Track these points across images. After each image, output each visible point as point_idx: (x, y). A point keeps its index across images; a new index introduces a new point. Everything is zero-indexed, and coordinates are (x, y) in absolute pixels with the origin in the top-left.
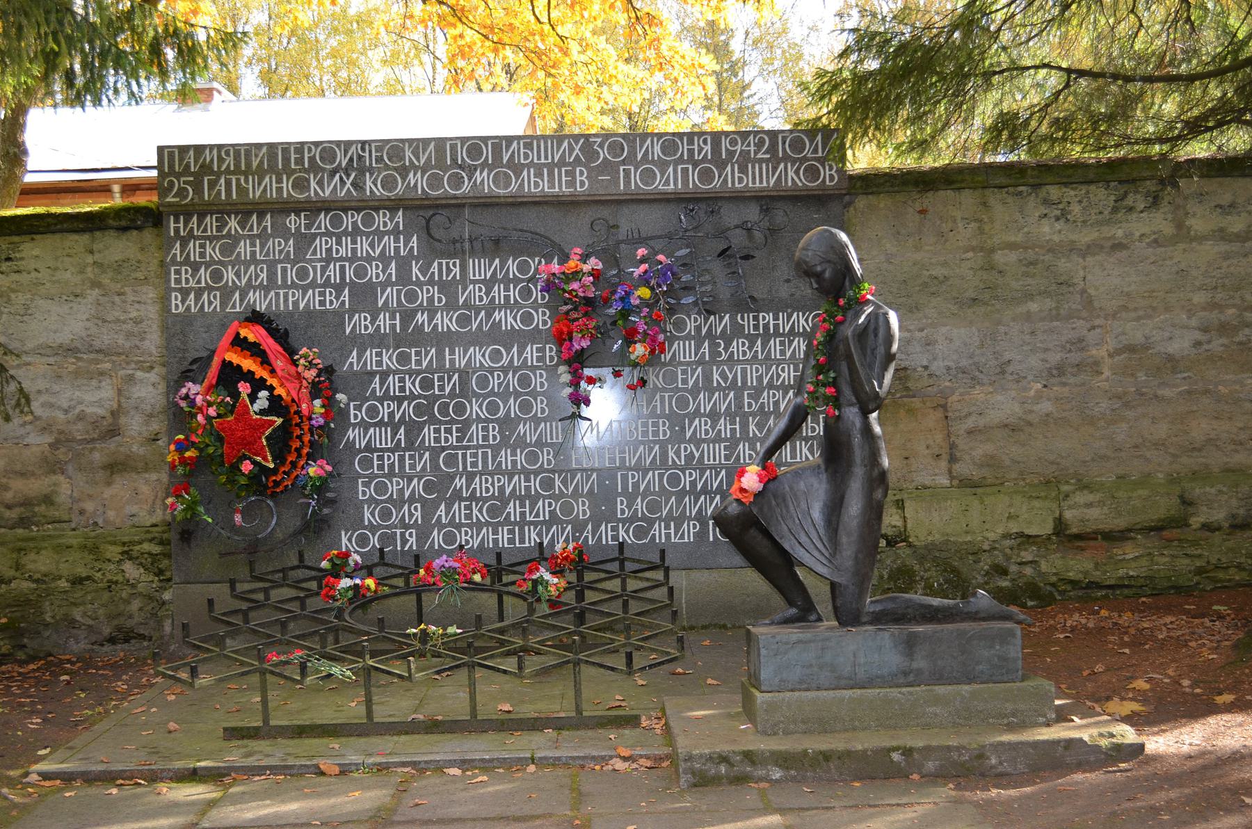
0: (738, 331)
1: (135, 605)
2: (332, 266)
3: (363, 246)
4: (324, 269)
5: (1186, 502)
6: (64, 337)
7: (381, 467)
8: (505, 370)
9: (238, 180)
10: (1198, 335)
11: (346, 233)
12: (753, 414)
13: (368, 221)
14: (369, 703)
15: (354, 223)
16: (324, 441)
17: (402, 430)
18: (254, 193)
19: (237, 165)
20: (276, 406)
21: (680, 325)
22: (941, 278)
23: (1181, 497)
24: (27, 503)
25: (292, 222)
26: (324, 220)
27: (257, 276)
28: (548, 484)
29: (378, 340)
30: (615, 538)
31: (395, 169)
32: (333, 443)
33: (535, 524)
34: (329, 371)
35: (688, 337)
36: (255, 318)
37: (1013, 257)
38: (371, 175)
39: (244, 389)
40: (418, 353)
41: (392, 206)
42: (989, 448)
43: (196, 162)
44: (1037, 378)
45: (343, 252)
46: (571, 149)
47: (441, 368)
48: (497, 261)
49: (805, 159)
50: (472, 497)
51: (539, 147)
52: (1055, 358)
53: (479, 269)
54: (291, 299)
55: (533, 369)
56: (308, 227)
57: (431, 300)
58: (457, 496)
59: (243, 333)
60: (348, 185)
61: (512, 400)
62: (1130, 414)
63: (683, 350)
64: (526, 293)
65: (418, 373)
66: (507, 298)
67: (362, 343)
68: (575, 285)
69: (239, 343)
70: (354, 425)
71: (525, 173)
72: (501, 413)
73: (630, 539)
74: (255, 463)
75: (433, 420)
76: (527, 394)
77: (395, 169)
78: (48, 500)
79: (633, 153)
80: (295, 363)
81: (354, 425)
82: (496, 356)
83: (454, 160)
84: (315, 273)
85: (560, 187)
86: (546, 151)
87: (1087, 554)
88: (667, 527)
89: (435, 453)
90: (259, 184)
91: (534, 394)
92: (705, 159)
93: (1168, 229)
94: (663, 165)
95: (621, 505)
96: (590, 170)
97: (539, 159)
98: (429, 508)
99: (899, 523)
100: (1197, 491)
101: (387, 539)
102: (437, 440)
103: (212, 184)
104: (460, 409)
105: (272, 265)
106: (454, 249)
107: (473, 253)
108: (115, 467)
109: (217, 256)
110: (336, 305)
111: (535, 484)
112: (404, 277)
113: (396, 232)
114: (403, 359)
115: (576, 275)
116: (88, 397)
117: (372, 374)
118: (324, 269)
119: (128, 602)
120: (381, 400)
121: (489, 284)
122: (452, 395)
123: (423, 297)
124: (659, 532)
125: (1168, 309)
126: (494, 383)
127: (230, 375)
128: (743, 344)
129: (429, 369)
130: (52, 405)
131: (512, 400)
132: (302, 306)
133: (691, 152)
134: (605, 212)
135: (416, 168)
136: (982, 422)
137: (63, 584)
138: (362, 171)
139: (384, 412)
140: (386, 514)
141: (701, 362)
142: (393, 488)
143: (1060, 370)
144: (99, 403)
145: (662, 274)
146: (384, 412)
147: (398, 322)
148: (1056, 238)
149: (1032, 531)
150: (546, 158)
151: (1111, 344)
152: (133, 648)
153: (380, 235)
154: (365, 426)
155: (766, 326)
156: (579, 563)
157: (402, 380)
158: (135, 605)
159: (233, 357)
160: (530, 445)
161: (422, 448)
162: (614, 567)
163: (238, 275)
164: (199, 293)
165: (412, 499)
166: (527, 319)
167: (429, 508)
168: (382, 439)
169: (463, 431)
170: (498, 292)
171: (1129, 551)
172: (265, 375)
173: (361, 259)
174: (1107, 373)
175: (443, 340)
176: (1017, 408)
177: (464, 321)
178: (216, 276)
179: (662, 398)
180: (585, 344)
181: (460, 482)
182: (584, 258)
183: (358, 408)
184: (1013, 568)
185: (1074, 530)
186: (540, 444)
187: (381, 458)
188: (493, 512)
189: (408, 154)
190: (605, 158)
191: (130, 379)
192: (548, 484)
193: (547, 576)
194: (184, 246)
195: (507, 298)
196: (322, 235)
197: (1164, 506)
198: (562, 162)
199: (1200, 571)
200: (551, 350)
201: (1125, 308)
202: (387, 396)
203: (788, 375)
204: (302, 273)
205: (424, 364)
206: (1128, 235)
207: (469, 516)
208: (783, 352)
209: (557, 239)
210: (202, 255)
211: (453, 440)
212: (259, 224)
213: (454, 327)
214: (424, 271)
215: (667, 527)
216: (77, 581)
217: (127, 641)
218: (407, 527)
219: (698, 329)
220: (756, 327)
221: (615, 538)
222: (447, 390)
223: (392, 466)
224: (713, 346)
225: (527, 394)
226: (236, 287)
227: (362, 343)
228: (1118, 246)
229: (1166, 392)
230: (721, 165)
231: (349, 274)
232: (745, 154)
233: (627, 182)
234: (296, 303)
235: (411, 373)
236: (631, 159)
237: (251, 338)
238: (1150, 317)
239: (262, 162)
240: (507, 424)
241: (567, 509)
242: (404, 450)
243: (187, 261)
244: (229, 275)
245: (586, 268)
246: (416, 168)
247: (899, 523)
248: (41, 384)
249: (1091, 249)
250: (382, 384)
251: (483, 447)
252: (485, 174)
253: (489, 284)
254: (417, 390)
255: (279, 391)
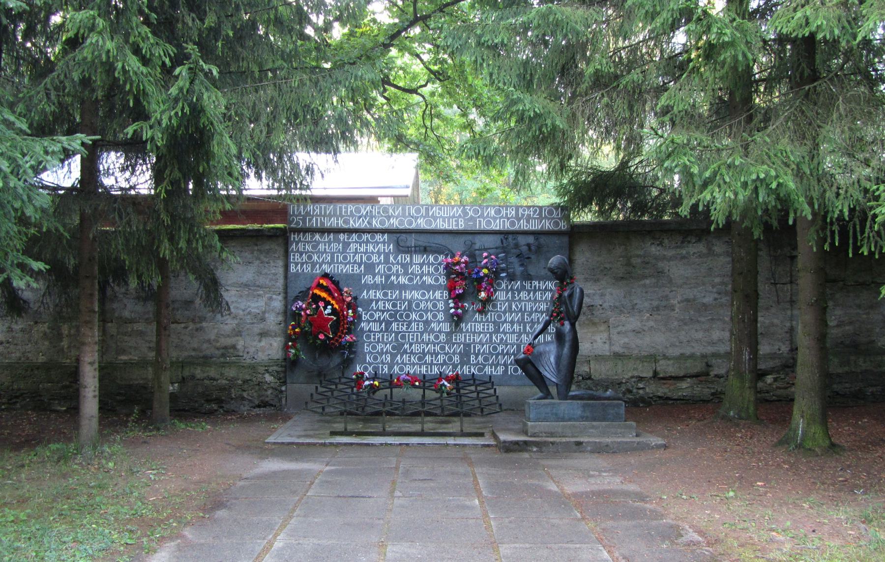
0: (523, 288)
1: (269, 392)
3: (370, 248)
4: (354, 257)
5: (708, 366)
6: (244, 280)
7: (374, 339)
8: (427, 301)
10: (716, 296)
11: (363, 242)
12: (529, 323)
13: (373, 238)
14: (424, 396)
16: (352, 327)
18: (327, 224)
19: (321, 212)
20: (334, 312)
21: (499, 285)
23: (707, 363)
24: (225, 348)
25: (342, 237)
26: (355, 236)
28: (443, 348)
29: (375, 286)
30: (470, 372)
32: (355, 329)
33: (437, 365)
34: (355, 298)
35: (503, 290)
36: (326, 276)
37: (639, 260)
39: (321, 304)
41: (383, 232)
42: (626, 340)
44: (648, 311)
47: (400, 299)
49: (553, 218)
50: (412, 353)
52: (655, 303)
53: (418, 259)
55: (438, 300)
56: (348, 239)
57: (397, 271)
58: (405, 352)
59: (321, 281)
62: (686, 328)
63: (500, 296)
64: (437, 270)
65: (391, 300)
67: (369, 287)
68: (457, 267)
69: (320, 286)
72: (425, 318)
73: (476, 372)
74: (325, 335)
75: (396, 320)
78: (234, 347)
79: (483, 214)
80: (342, 295)
82: (423, 295)
83: (409, 214)
84: (350, 257)
85: (452, 226)
87: (666, 386)
89: (397, 333)
91: (438, 311)
92: (512, 217)
93: (705, 251)
94: (495, 219)
95: (473, 358)
96: (465, 220)
98: (393, 356)
99: (588, 370)
100: (714, 361)
101: (376, 369)
102: (398, 328)
103: (310, 220)
104: (408, 316)
105: (333, 254)
106: (408, 250)
107: (415, 252)
108: (263, 334)
109: (310, 249)
111: (437, 348)
112: (387, 261)
113: (384, 242)
114: (385, 294)
115: (458, 263)
116: (253, 305)
117: (372, 301)
118: (354, 257)
119: (266, 390)
121: (422, 265)
122: (405, 310)
123: (394, 269)
124: (488, 370)
125: (704, 284)
126: (422, 306)
127: (316, 299)
129: (396, 299)
130: (237, 308)
133: (507, 214)
134: (470, 237)
136: (624, 329)
137: (240, 382)
138: (372, 217)
139: (376, 316)
140: (375, 358)
141: (507, 300)
142: (379, 348)
143: (658, 308)
144: (257, 308)
145: (492, 264)
146: (376, 316)
148: (658, 253)
149: (644, 375)
151: (679, 298)
152: (272, 408)
153: (378, 243)
154: (369, 322)
155: (535, 287)
156: (455, 379)
157: (384, 303)
158: (269, 392)
159: (317, 291)
161: (392, 332)
162: (471, 382)
163: (318, 257)
164: (302, 264)
165: (387, 352)
166: (437, 280)
167: (393, 356)
168: (375, 327)
169: (409, 325)
170: (425, 269)
171: (684, 385)
172: (330, 299)
174: (677, 310)
175: (402, 287)
176: (639, 324)
177: (411, 280)
178: (310, 258)
180: (461, 291)
181: (406, 346)
182: (461, 256)
183: (366, 314)
184: (635, 391)
185: (661, 376)
186: (440, 332)
187: (374, 335)
188: (420, 359)
189: (391, 211)
191: (270, 299)
192: (443, 348)
193: (446, 383)
194: (297, 245)
197: (698, 367)
198: (454, 216)
199: (713, 394)
200: (446, 294)
201: (685, 283)
202: (378, 310)
203: (543, 307)
204: (345, 258)
206: (688, 253)
207: (410, 360)
209: (450, 247)
210: (304, 249)
211: (404, 329)
213: (407, 282)
214: (395, 258)
216: (245, 381)
217: (265, 407)
218: (384, 364)
219: (507, 286)
221: (470, 372)
223: (379, 338)
224: (513, 294)
226: (317, 262)
227: (369, 287)
228: (683, 257)
229: (703, 319)
230: (519, 220)
231: (364, 259)
232: (529, 215)
233: (480, 225)
234: (342, 270)
235: (388, 300)
236: (482, 216)
237: (325, 284)
238: (695, 287)
240: (427, 323)
241: (450, 359)
243: (298, 251)
244: (315, 257)
245: (463, 260)
247: (588, 370)
248: (234, 299)
249: (670, 259)
253: (422, 265)
255: (336, 306)
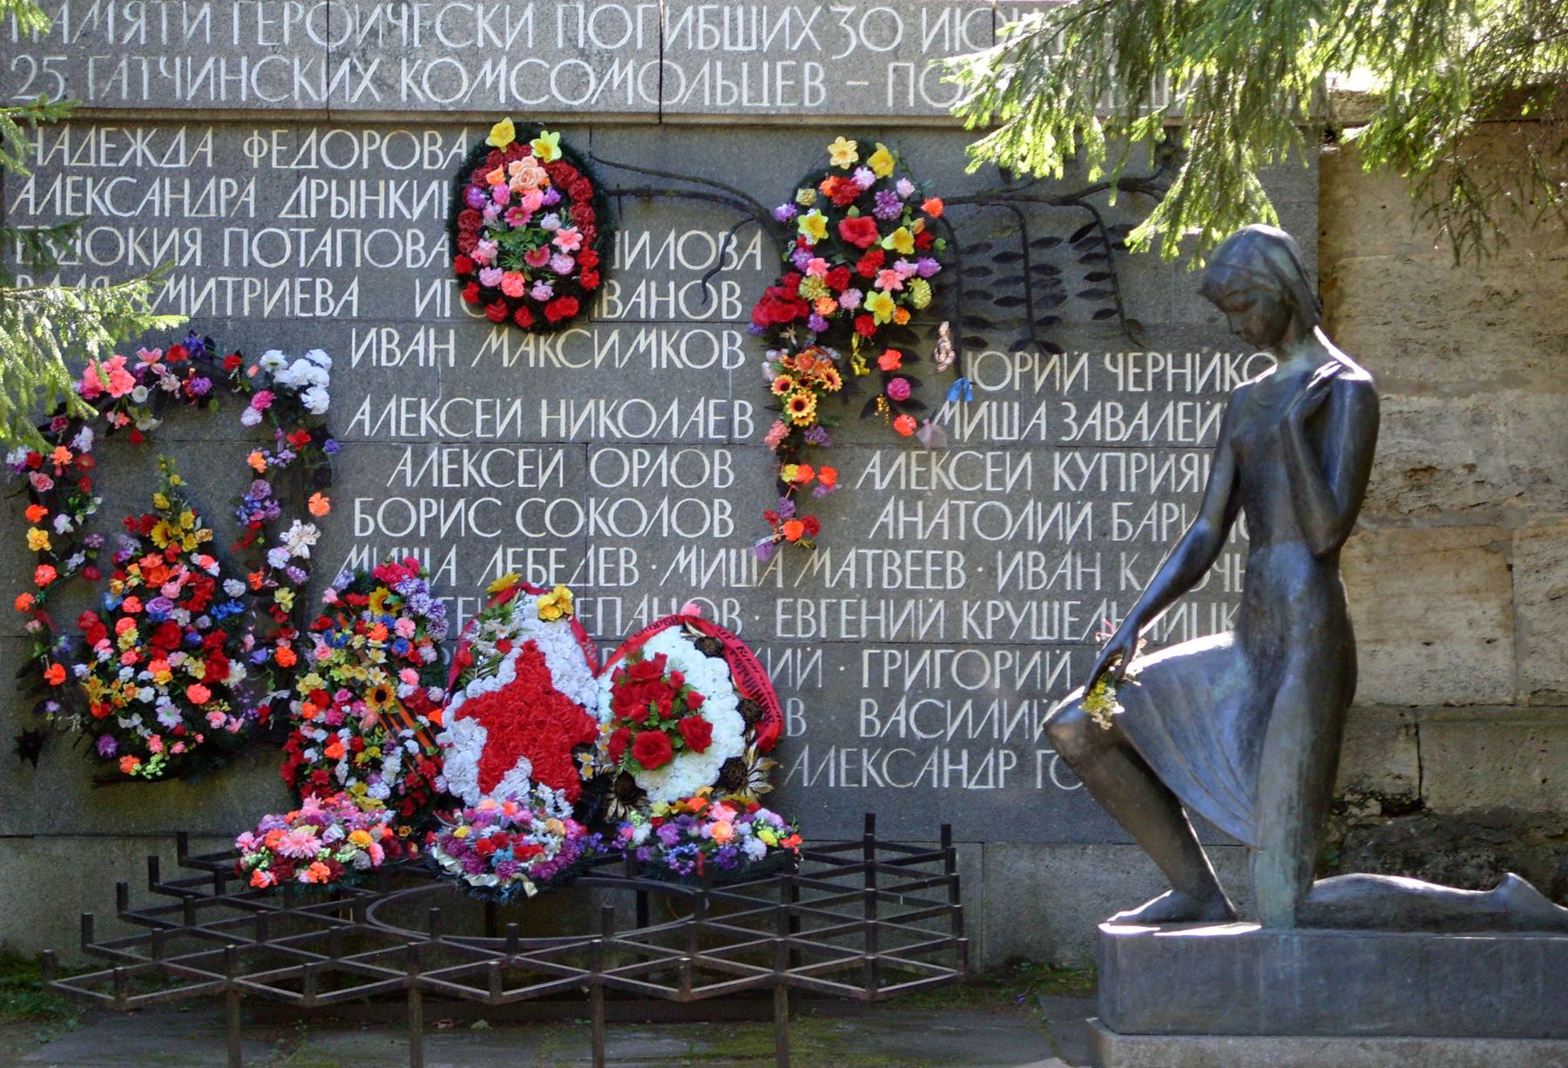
0: (1103, 386)
2: (328, 236)
3: (392, 198)
8: (653, 445)
9: (154, 66)
11: (356, 172)
13: (401, 152)
15: (375, 155)
17: (452, 554)
19: (153, 32)
22: (1509, 294)
25: (258, 148)
26: (315, 144)
27: (184, 249)
29: (413, 380)
31: (457, 54)
35: (1007, 395)
38: (411, 62)
40: (488, 409)
43: (73, 25)
45: (350, 208)
46: (796, 28)
48: (646, 236)
51: (733, 20)
54: (247, 296)
55: (708, 445)
56: (285, 158)
60: (366, 82)
61: (665, 504)
65: (487, 444)
66: (662, 307)
70: (361, 543)
71: (706, 69)
72: (643, 527)
75: (511, 537)
76: (693, 493)
77: (457, 54)
79: (914, 38)
81: (361, 543)
83: (571, 40)
86: (747, 28)
88: (955, 759)
90: (196, 73)
91: (708, 494)
96: (831, 68)
97: (734, 42)
103: (104, 71)
104: (565, 517)
110: (334, 310)
114: (461, 417)
118: (313, 241)
120: (415, 496)
122: (551, 490)
124: (940, 769)
128: (1114, 412)
129: (509, 440)
131: (665, 504)
132: (267, 309)
135: (495, 53)
138: (394, 58)
146: (419, 517)
147: (451, 346)
150: (747, 42)
155: (1160, 379)
157: (455, 458)
160: (696, 591)
163: (146, 245)
166: (700, 349)
173: (385, 222)
179: (954, 510)
183: (371, 509)
190: (860, 46)
194: (43, 186)
195: (662, 307)
196: (312, 174)
198: (777, 52)
202: (425, 489)
204: (271, 247)
205: (500, 430)
208: (1190, 430)
212: (190, 149)
215: (955, 759)
219: (1028, 379)
220: (1140, 380)
222: (542, 480)
224: (1057, 412)
225: (693, 493)
231: (362, 251)
233: (901, 94)
234: (257, 304)
235: (471, 444)
239: (201, 30)
240: (656, 547)
242: (456, 592)
246: (495, 53)
250: (416, 466)
251: (606, 591)
252: (629, 69)
254: (484, 479)
